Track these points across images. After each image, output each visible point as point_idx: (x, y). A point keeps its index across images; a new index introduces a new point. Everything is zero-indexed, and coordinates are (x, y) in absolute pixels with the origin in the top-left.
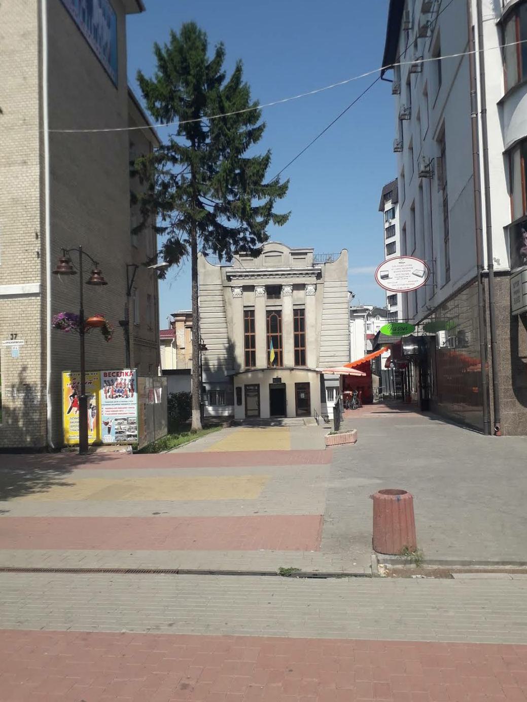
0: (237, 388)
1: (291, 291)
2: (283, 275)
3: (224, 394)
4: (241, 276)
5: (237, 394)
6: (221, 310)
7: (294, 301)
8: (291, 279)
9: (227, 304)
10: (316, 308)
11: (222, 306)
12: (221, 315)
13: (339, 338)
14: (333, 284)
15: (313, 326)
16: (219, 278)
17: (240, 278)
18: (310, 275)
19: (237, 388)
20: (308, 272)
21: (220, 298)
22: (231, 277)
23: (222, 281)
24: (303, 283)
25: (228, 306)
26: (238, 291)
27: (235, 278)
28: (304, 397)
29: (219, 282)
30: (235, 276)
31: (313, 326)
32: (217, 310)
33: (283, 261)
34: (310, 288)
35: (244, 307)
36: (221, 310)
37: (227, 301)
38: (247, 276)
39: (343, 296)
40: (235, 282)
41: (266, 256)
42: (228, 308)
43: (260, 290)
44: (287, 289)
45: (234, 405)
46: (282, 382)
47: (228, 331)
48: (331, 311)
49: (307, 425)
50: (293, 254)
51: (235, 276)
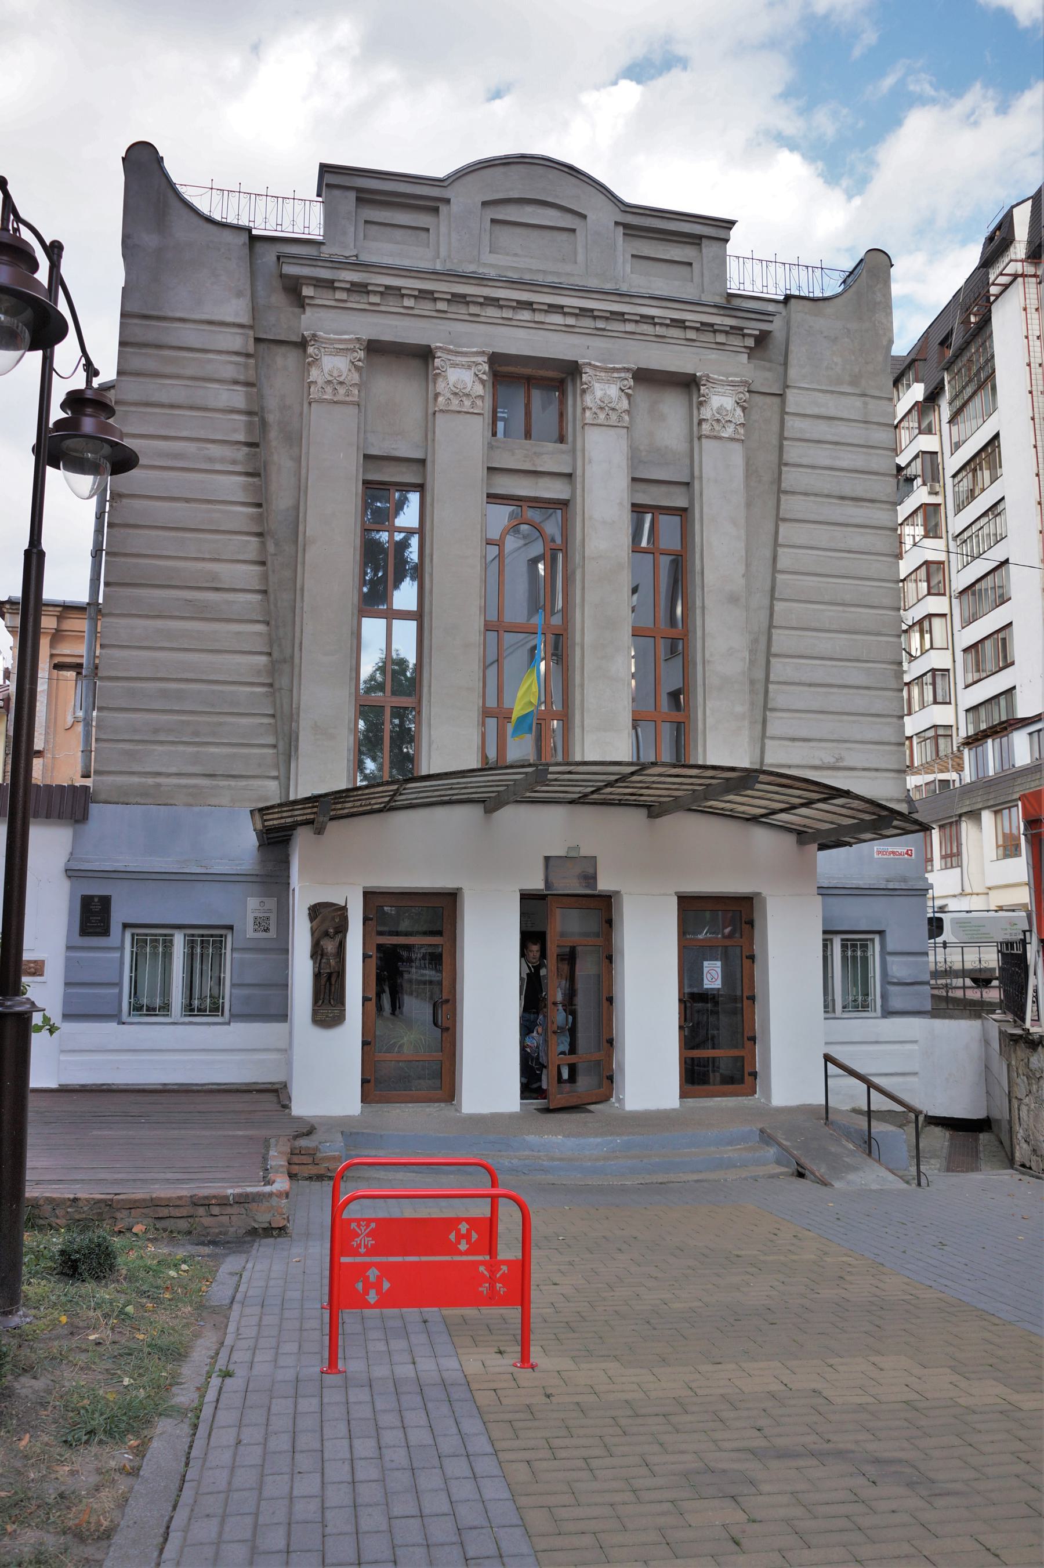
0: (315, 911)
1: (625, 404)
2: (584, 312)
3: (219, 944)
4: (360, 289)
5: (317, 952)
6: (234, 462)
7: (634, 458)
8: (631, 345)
9: (273, 434)
10: (749, 505)
11: (241, 437)
12: (232, 486)
13: (855, 675)
14: (830, 405)
15: (733, 599)
16: (239, 294)
17: (356, 301)
18: (721, 338)
19: (315, 911)
20: (716, 320)
21: (237, 398)
22: (307, 291)
23: (254, 310)
24: (689, 370)
25: (274, 444)
26: (334, 365)
27: (325, 298)
28: (718, 984)
29: (235, 310)
30: (329, 285)
31: (733, 599)
32: (211, 460)
33: (581, 258)
34: (721, 401)
35: (367, 457)
36: (234, 462)
37: (271, 418)
38: (396, 292)
39: (874, 466)
40: (323, 321)
41: (493, 221)
42: (280, 460)
43: (462, 377)
44: (603, 391)
45: (283, 1016)
46: (604, 885)
47: (265, 577)
48: (822, 536)
49: (837, 1185)
50: (630, 231)
51: (329, 285)
